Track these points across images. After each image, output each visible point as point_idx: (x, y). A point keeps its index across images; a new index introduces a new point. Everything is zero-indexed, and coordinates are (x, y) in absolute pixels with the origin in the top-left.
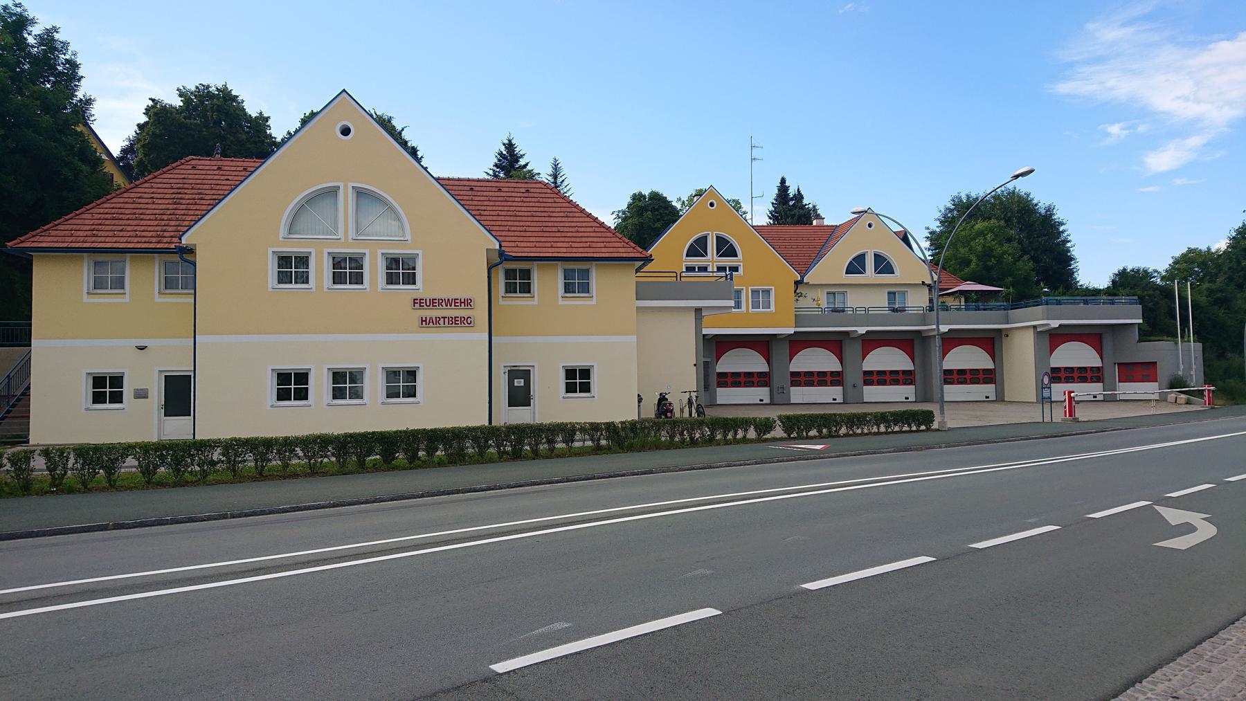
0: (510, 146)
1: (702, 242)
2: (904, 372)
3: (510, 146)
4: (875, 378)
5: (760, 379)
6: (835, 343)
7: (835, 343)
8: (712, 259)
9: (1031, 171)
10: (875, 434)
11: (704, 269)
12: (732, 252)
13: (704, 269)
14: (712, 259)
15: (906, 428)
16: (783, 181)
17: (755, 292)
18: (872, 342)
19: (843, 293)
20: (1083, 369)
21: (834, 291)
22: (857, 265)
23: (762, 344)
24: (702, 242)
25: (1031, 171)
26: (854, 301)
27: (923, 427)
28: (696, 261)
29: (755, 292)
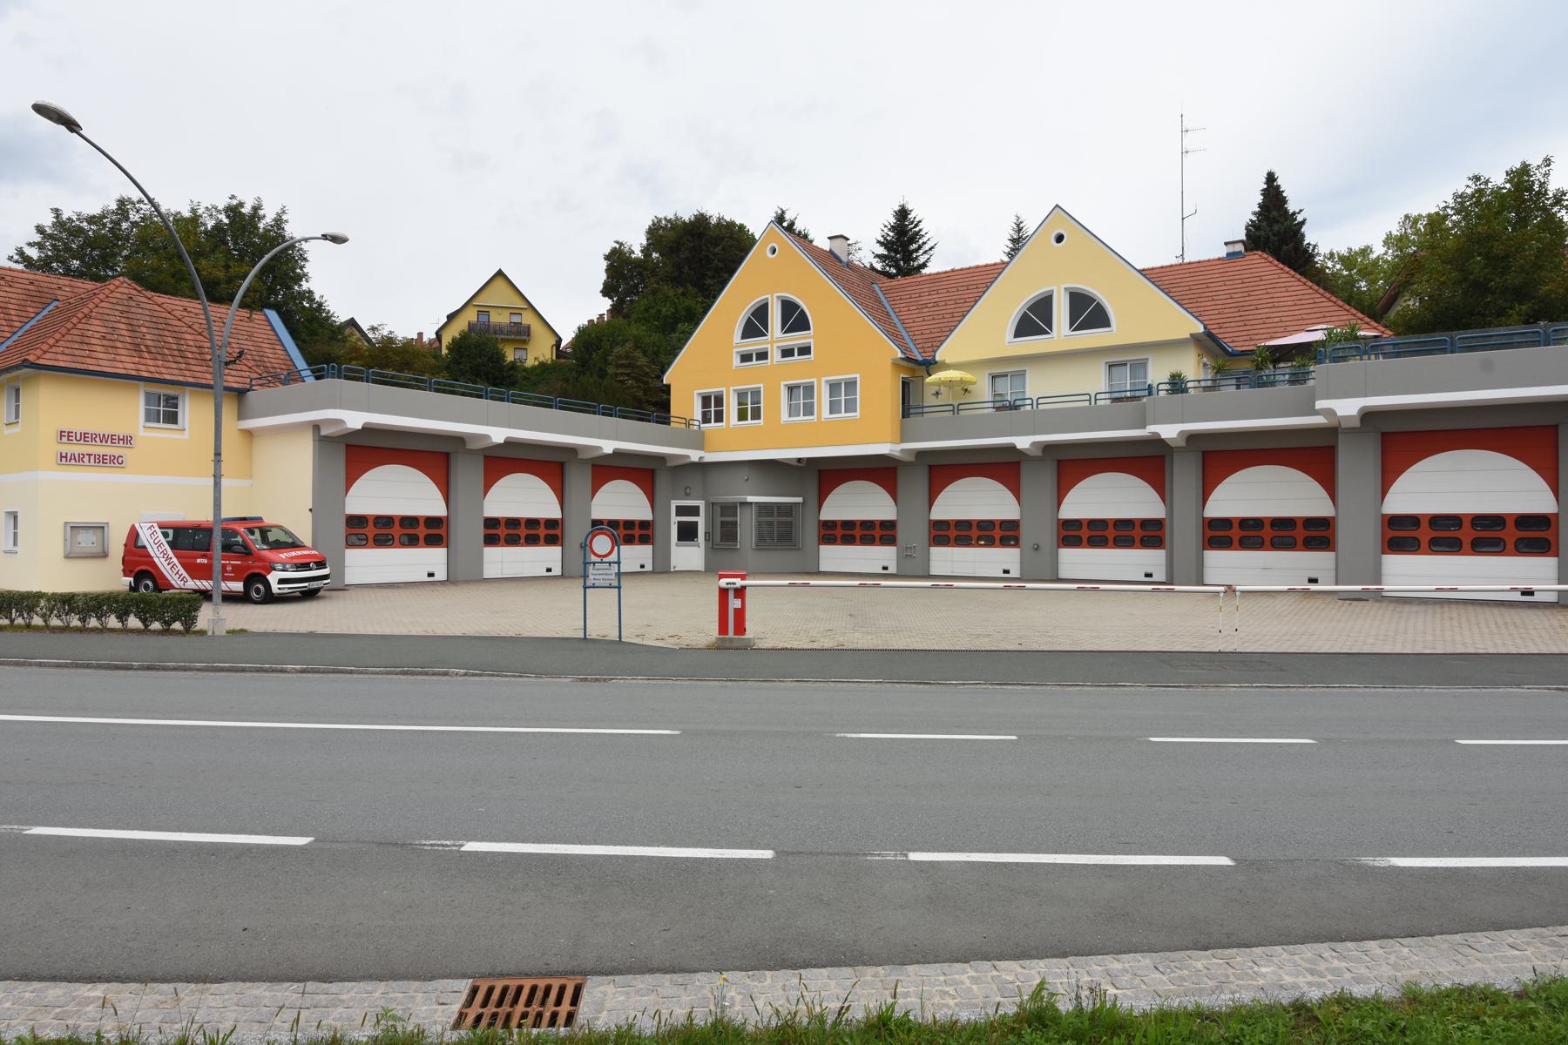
0: (903, 214)
1: (761, 313)
2: (1145, 523)
3: (903, 214)
4: (953, 533)
5: (430, 532)
6: (1003, 467)
7: (1003, 467)
8: (776, 335)
9: (40, 109)
10: (77, 629)
11: (763, 355)
13: (763, 355)
14: (776, 335)
15: (93, 622)
16: (1271, 178)
18: (1074, 464)
19: (1015, 375)
20: (532, 523)
21: (1005, 370)
22: (1035, 319)
23: (881, 471)
24: (761, 313)
25: (40, 109)
26: (1039, 386)
27: (177, 626)
28: (754, 345)
29: (834, 387)
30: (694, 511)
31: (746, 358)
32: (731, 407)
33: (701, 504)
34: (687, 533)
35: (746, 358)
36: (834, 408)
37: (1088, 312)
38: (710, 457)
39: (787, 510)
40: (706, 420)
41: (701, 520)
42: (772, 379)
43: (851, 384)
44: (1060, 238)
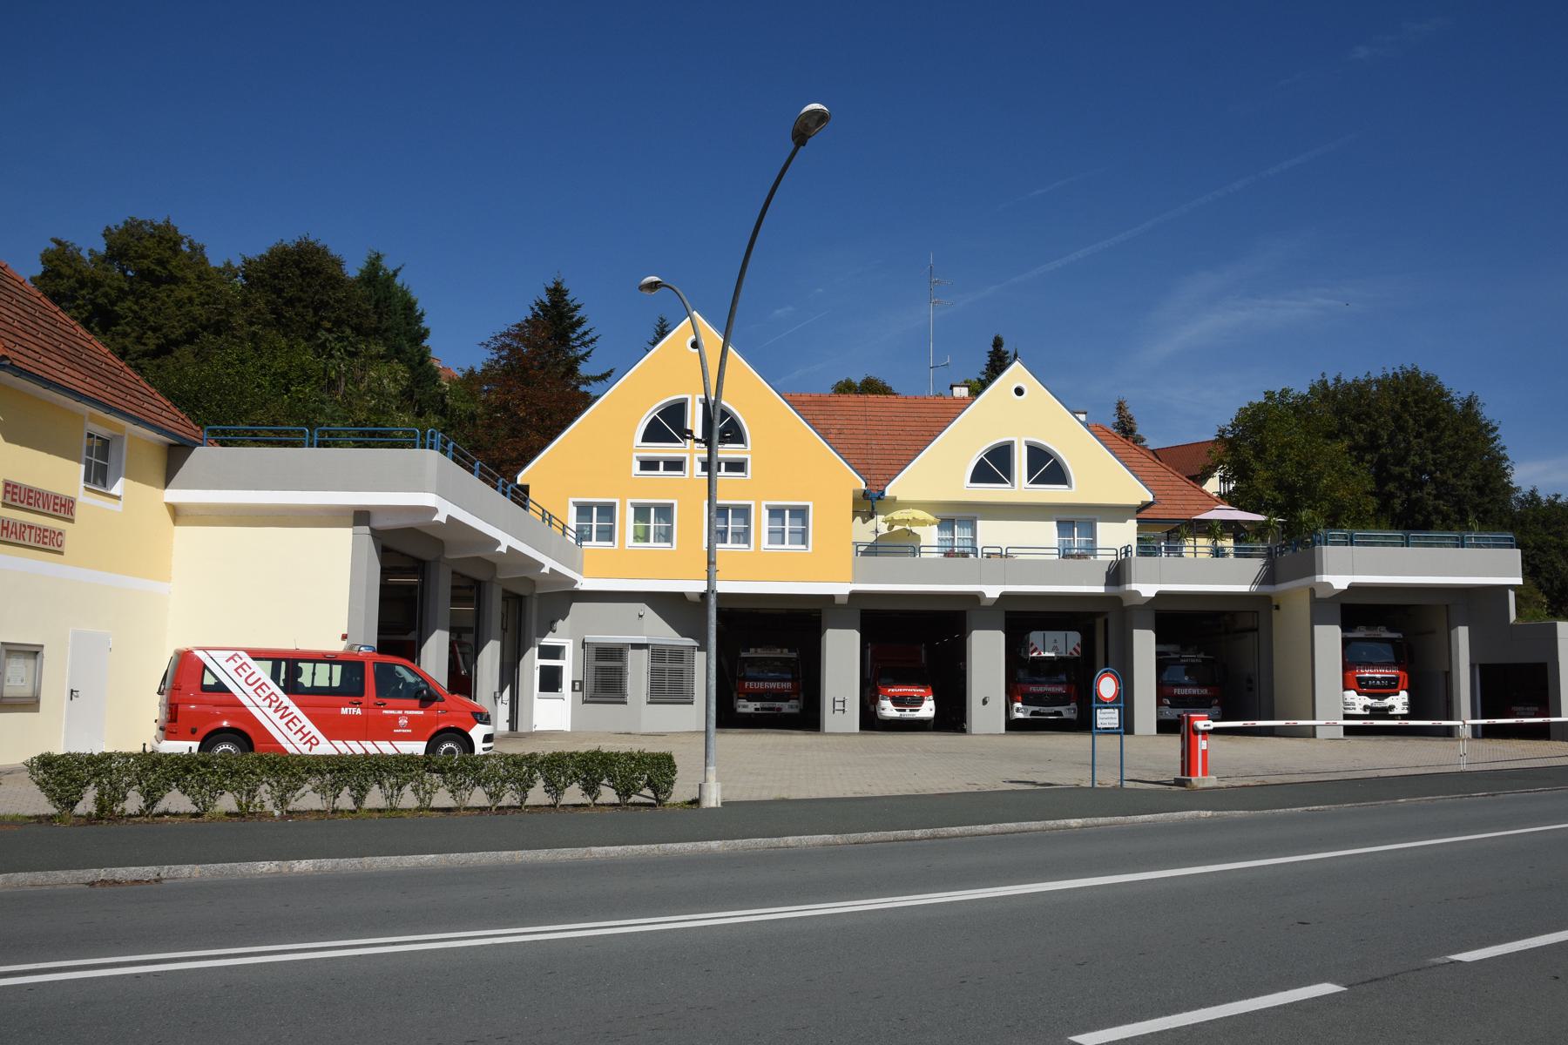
11: (675, 465)
12: (734, 433)
13: (675, 465)
17: (776, 513)
21: (955, 516)
22: (995, 465)
30: (555, 652)
31: (648, 465)
32: (626, 521)
33: (570, 646)
34: (550, 681)
35: (648, 465)
36: (777, 535)
37: (1047, 467)
38: (585, 584)
39: (678, 654)
40: (582, 536)
41: (569, 667)
42: (685, 491)
43: (800, 513)
44: (1019, 392)
